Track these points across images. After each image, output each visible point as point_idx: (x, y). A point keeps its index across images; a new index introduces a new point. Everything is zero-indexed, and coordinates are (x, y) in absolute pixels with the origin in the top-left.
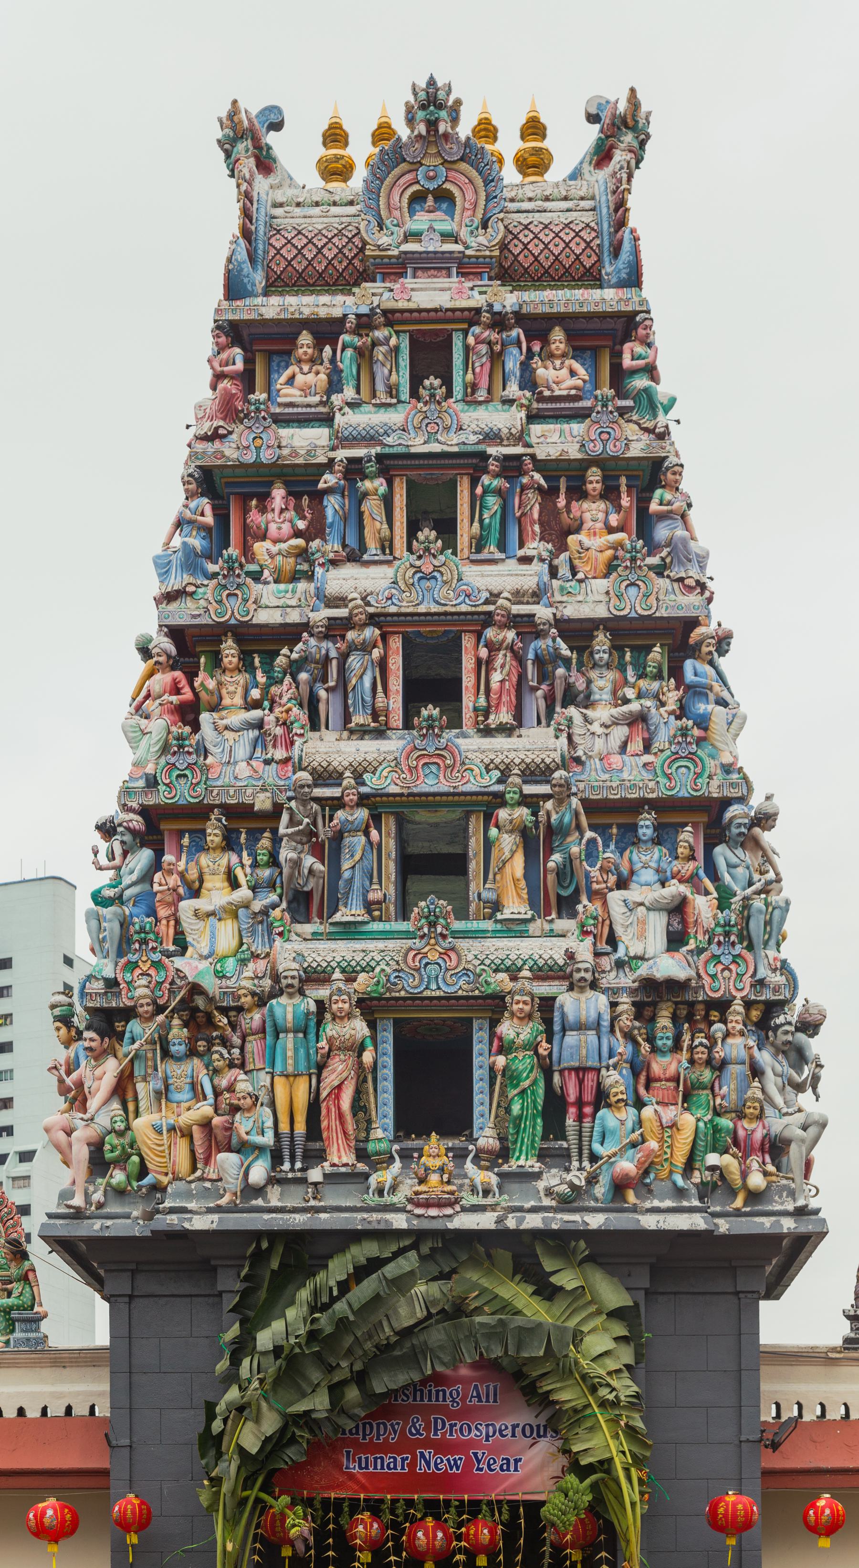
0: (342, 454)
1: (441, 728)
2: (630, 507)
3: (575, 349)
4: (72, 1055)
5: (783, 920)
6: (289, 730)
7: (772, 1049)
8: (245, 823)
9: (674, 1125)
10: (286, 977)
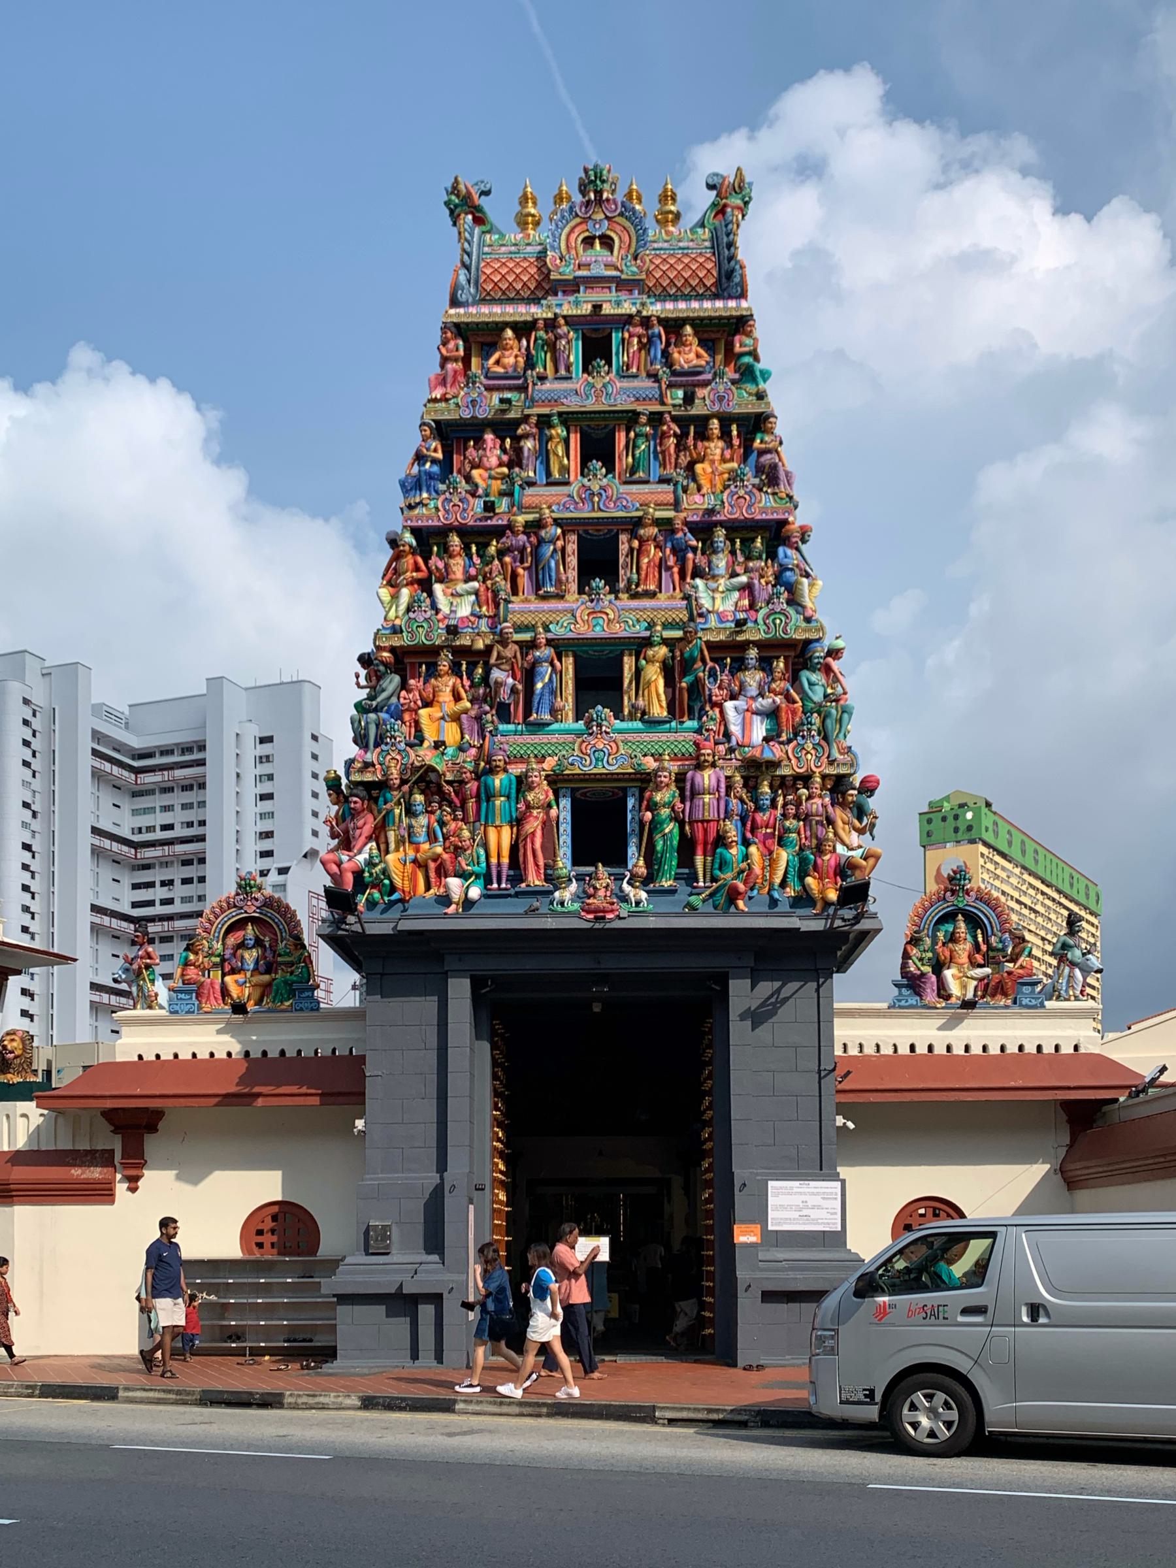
8: (468, 659)
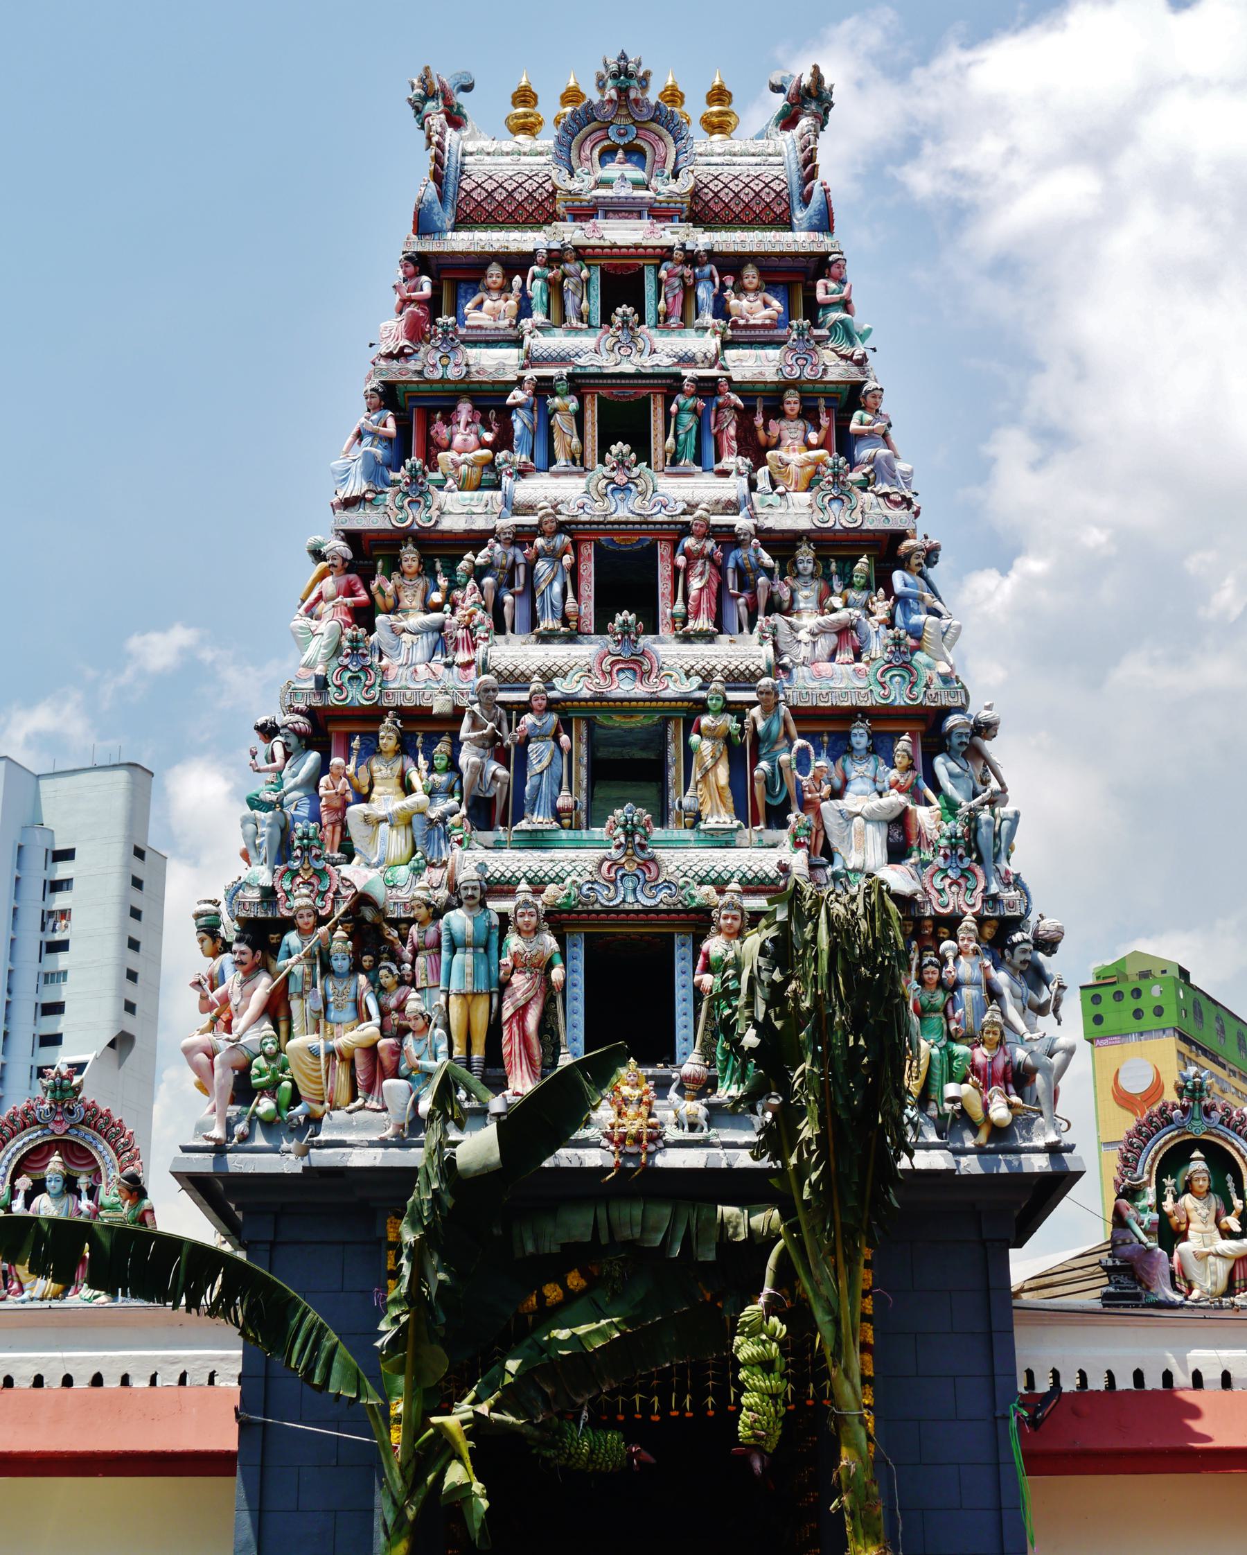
0: (530, 374)
1: (638, 635)
2: (830, 427)
3: (767, 283)
4: (217, 969)
5: (1012, 832)
6: (472, 633)
7: (1010, 969)
8: (424, 729)
10: (466, 888)
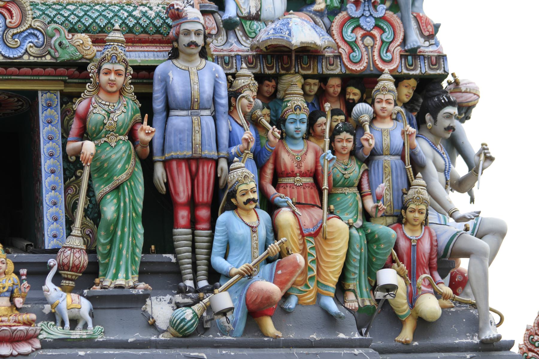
9: (318, 233)
